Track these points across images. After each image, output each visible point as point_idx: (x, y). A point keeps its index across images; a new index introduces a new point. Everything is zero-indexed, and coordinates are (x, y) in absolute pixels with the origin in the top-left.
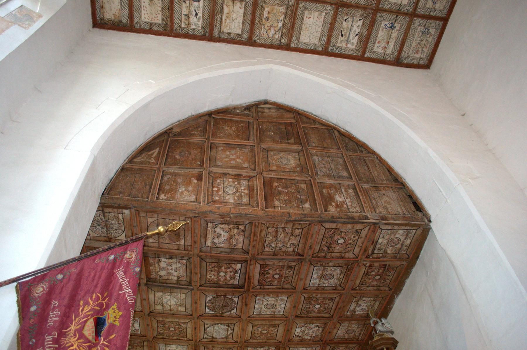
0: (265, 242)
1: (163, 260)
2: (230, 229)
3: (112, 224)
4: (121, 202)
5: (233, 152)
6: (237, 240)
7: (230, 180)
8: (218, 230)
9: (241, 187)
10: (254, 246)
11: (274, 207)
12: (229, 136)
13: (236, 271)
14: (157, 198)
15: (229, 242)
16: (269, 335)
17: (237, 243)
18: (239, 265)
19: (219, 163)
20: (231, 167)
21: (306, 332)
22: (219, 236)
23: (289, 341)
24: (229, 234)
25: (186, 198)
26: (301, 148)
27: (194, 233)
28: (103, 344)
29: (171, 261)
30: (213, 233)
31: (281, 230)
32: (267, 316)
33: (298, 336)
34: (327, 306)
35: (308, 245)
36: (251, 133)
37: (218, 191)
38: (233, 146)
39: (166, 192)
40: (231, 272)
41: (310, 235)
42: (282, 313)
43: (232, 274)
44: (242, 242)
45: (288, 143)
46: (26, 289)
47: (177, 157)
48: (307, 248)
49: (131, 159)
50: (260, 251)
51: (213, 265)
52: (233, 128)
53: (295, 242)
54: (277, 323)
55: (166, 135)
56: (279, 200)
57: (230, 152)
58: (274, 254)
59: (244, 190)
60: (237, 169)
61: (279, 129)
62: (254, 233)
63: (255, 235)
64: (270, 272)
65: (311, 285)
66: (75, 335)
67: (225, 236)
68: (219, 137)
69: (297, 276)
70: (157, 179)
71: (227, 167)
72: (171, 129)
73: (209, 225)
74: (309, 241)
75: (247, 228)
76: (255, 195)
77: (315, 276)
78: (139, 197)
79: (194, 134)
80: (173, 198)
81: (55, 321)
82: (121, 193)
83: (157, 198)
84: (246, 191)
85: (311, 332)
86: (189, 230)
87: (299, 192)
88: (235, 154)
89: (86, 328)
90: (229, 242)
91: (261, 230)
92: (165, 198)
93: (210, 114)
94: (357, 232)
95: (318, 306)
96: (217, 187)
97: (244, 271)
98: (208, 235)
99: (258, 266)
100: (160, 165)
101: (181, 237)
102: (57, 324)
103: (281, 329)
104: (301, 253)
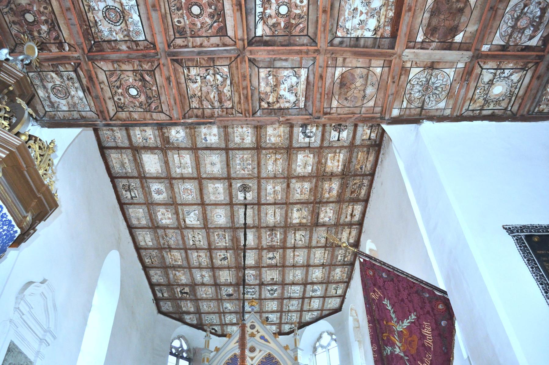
0: (231, 83)
1: (368, 34)
2: (278, 102)
3: (419, 91)
6: (267, 84)
8: (292, 98)
10: (244, 77)
13: (264, 18)
15: (277, 79)
17: (267, 77)
18: (259, 33)
22: (290, 90)
24: (278, 94)
27: (321, 94)
29: (359, 33)
30: (299, 93)
31: (217, 104)
35: (173, 83)
40: (270, 16)
41: (178, 101)
44: (261, 80)
48: (173, 78)
50: (234, 64)
51: (298, 29)
58: (213, 60)
62: (248, 101)
63: (247, 98)
64: (209, 21)
67: (283, 91)
69: (163, 11)
73: (303, 104)
74: (174, 91)
75: (258, 105)
86: (327, 94)
90: (277, 79)
94: (121, 108)
97: (249, 18)
98: (305, 89)
99: (230, 33)
101: (338, 81)
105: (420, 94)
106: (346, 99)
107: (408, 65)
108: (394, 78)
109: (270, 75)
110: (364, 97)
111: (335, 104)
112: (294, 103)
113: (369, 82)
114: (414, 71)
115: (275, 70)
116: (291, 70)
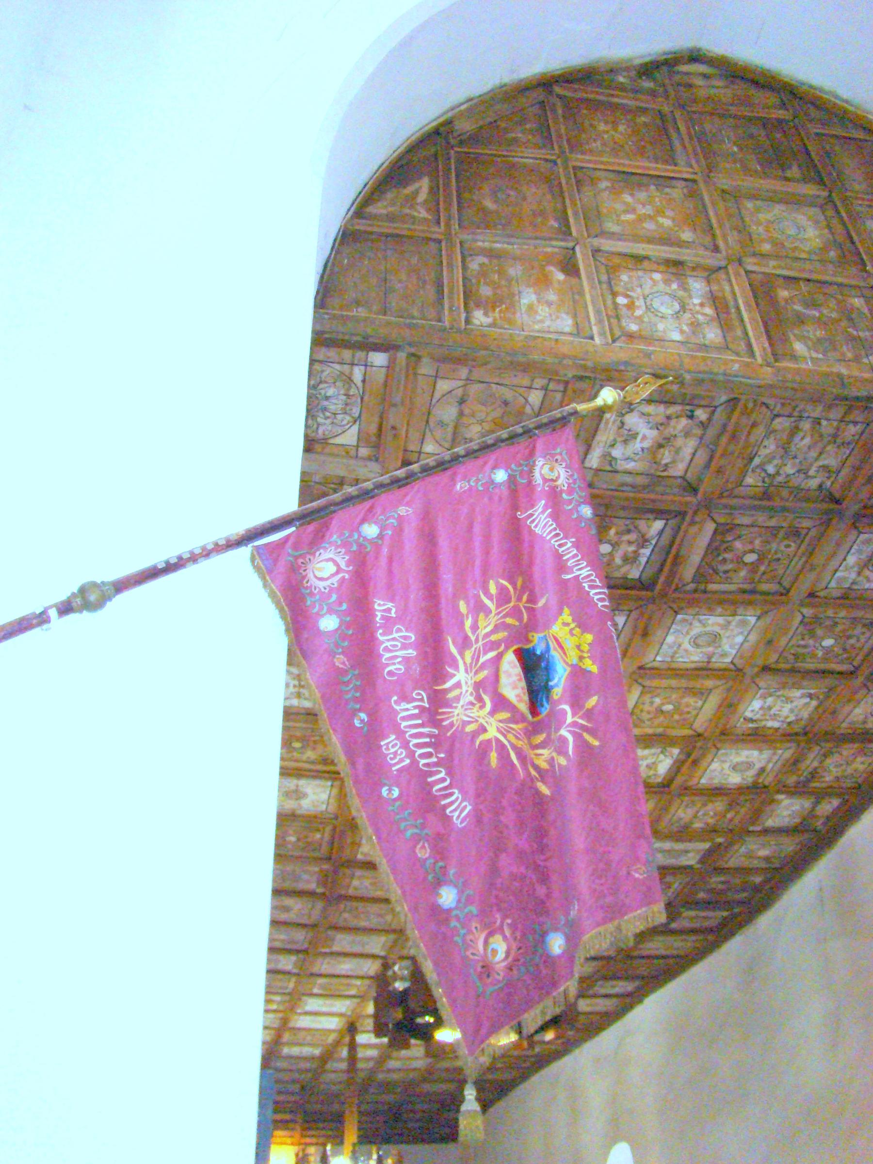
0: (751, 459)
2: (669, 418)
3: (327, 398)
4: (370, 331)
5: (642, 195)
6: (678, 451)
7: (657, 276)
9: (690, 297)
11: (794, 357)
12: (616, 149)
13: (644, 541)
14: (468, 321)
16: (676, 717)
18: (659, 524)
19: (611, 227)
20: (650, 241)
21: (772, 712)
23: (723, 733)
25: (547, 323)
26: (825, 194)
28: (574, 724)
30: (615, 428)
31: (806, 425)
32: (689, 666)
33: (751, 720)
34: (852, 641)
36: (677, 143)
37: (631, 306)
38: (636, 179)
39: (489, 305)
40: (630, 543)
42: (729, 660)
43: (632, 548)
44: (688, 458)
45: (786, 179)
46: (281, 567)
47: (489, 204)
49: (362, 208)
52: (621, 128)
53: (832, 462)
54: (709, 683)
55: (440, 140)
56: (803, 339)
57: (632, 195)
59: (702, 305)
60: (663, 245)
61: (751, 136)
63: (734, 437)
64: (738, 544)
65: (833, 584)
66: (480, 699)
68: (591, 151)
70: (450, 266)
71: (636, 238)
72: (449, 122)
76: (736, 323)
77: (851, 560)
78: (413, 318)
79: (515, 140)
80: (510, 321)
81: (406, 660)
82: (358, 303)
83: (468, 321)
84: (709, 311)
85: (785, 711)
87: (851, 319)
88: (650, 201)
89: (504, 680)
90: (654, 458)
91: (754, 425)
92: (489, 320)
93: (546, 83)
95: (828, 642)
96: (627, 296)
99: (710, 527)
100: (448, 225)
102: (416, 669)
103: (713, 702)
104: (837, 495)
105: (323, 392)
106: (506, 403)
107: (364, 452)
108: (395, 435)
109: (666, 465)
110: (462, 401)
111: (535, 398)
112: (632, 411)
113: (450, 430)
114: (350, 437)
115: (653, 471)
116: (619, 468)
